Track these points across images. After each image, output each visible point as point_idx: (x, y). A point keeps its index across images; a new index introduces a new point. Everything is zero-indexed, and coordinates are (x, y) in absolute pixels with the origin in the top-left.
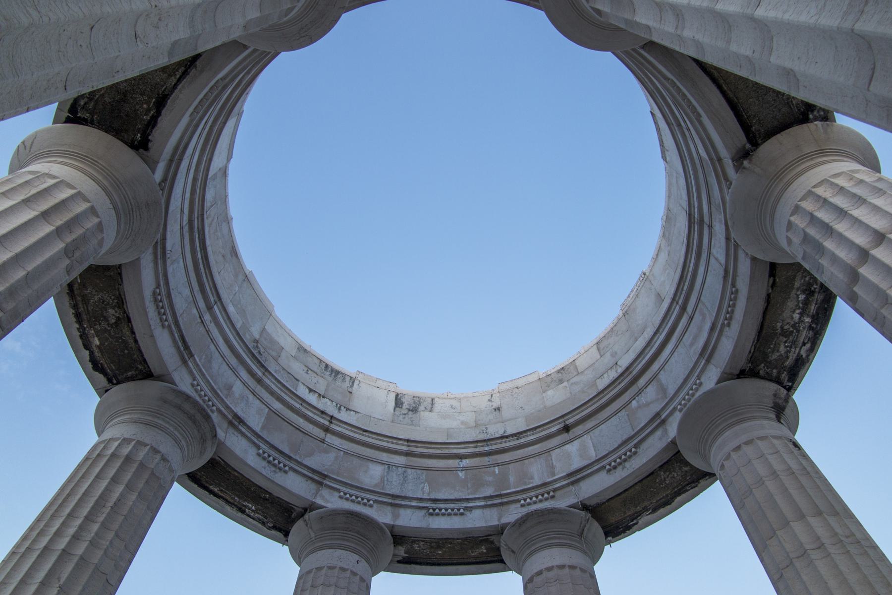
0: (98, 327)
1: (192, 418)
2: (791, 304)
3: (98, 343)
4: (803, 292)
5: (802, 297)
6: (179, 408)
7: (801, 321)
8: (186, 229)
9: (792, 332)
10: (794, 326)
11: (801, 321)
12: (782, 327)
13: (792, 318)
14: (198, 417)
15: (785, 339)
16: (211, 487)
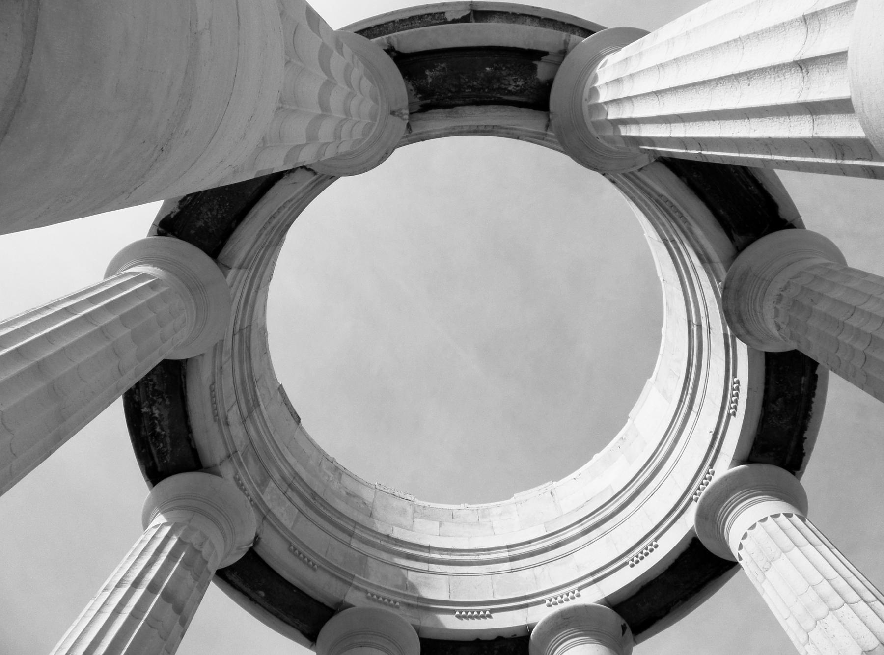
0: (796, 393)
1: (741, 320)
2: (166, 423)
3: (803, 378)
4: (159, 434)
5: (158, 429)
6: (749, 333)
7: (150, 406)
8: (695, 408)
9: (153, 395)
10: (154, 402)
11: (150, 406)
12: (164, 400)
13: (158, 409)
14: (734, 318)
15: (156, 388)
16: (757, 192)
